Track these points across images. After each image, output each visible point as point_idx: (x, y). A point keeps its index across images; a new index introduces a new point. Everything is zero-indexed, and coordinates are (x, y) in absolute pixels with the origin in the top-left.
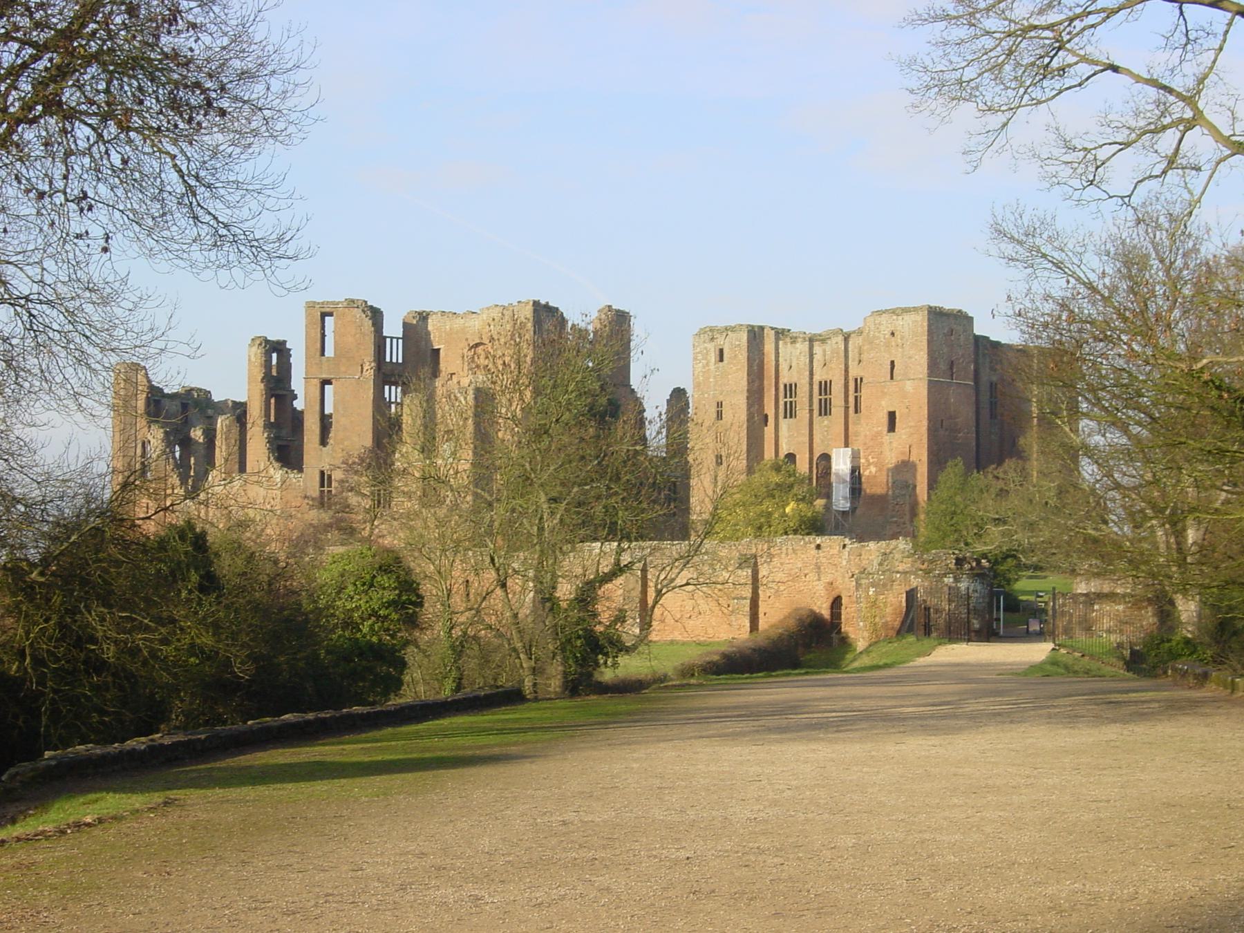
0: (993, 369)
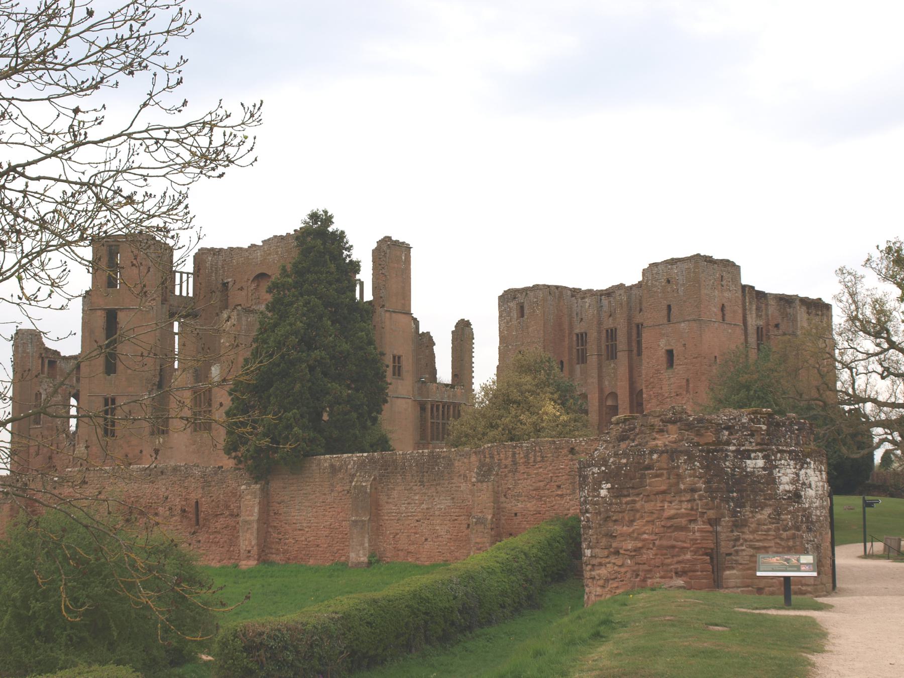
0: (759, 316)
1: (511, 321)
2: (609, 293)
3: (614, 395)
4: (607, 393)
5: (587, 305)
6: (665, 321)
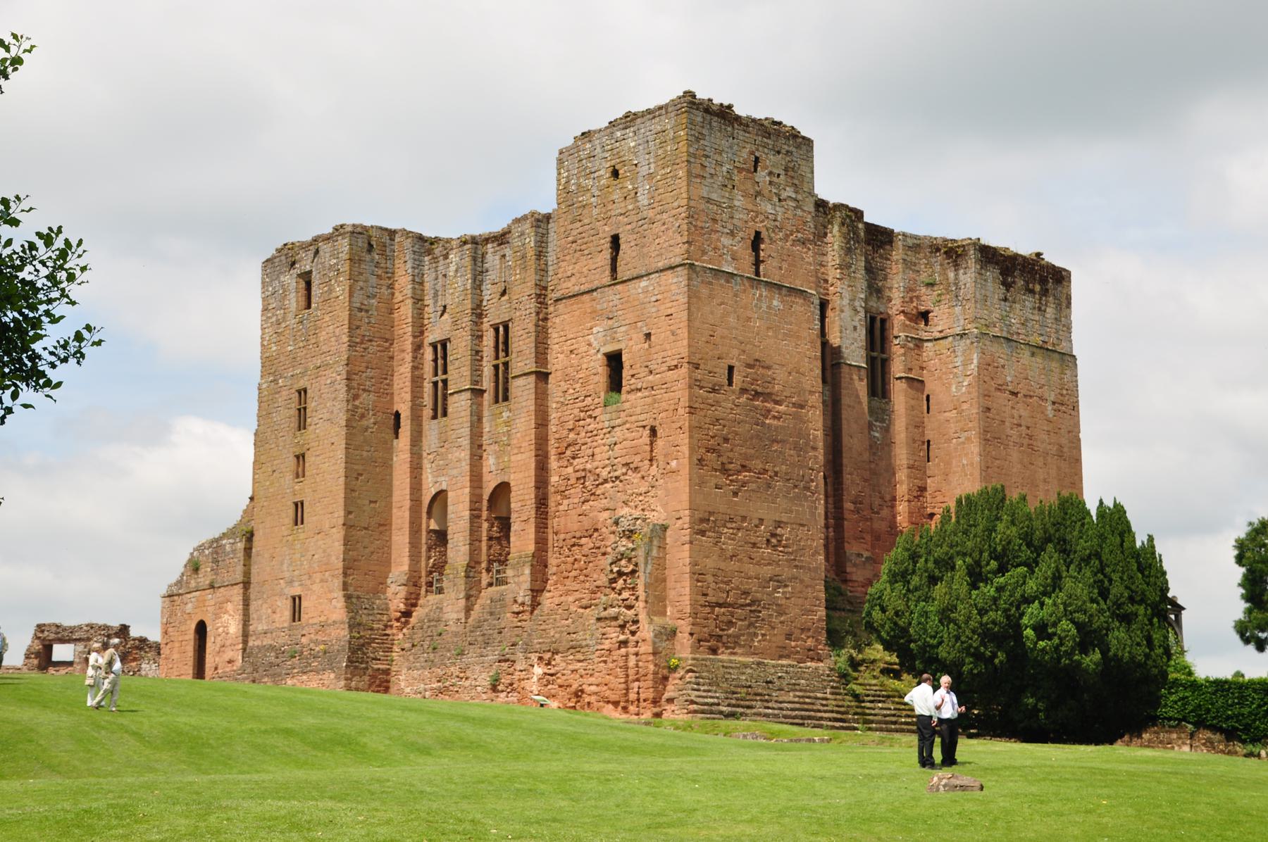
1: (284, 320)
2: (501, 239)
4: (492, 485)
5: (453, 268)
6: (607, 279)
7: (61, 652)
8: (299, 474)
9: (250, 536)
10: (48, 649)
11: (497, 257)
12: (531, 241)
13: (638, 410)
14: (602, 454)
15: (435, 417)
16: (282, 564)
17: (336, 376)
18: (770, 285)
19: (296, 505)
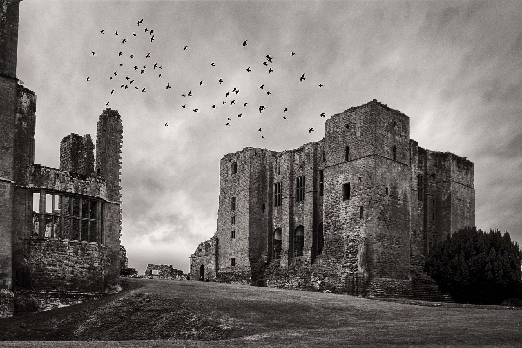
2: (300, 150)
3: (301, 228)
4: (296, 226)
5: (283, 160)
7: (155, 272)
8: (233, 222)
9: (217, 241)
10: (151, 271)
11: (298, 156)
12: (312, 151)
13: (356, 202)
14: (342, 216)
15: (276, 206)
16: (228, 249)
17: (246, 193)
18: (397, 162)
19: (232, 232)
